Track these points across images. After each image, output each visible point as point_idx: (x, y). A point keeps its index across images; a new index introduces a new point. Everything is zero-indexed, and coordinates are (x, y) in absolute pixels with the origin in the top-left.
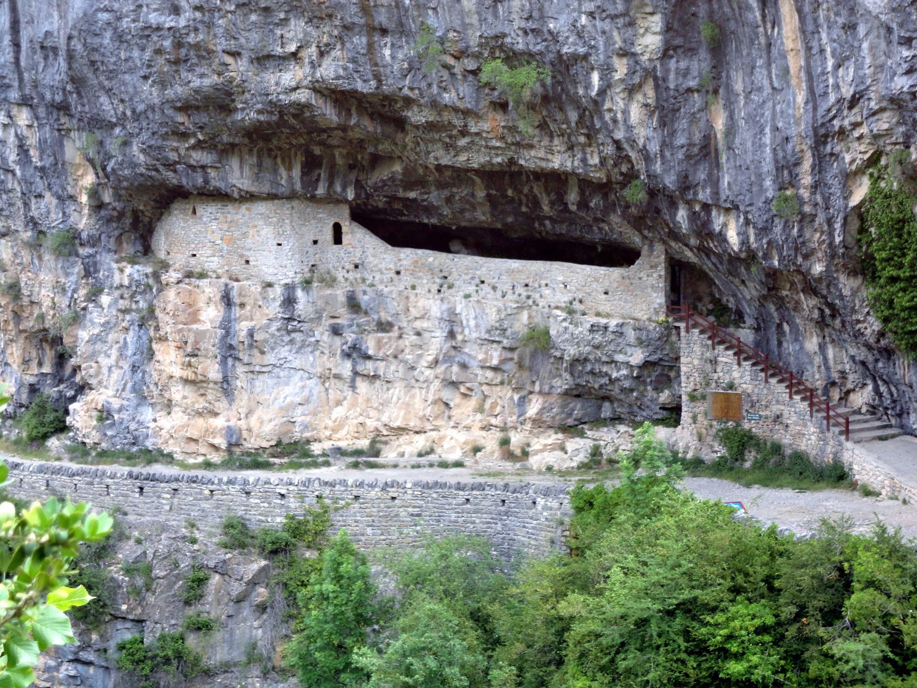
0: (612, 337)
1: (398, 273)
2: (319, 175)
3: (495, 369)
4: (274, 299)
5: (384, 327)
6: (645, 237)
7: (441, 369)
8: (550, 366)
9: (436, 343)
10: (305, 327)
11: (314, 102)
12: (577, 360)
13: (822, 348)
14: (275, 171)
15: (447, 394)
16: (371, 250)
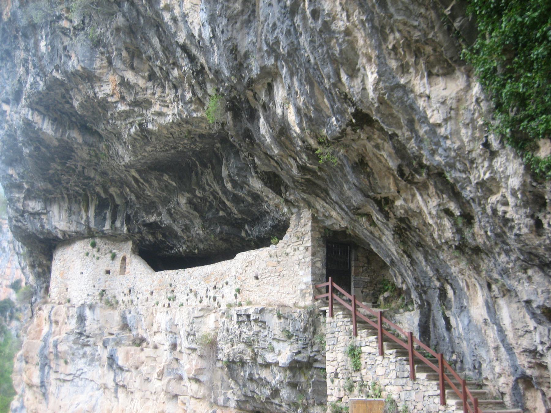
0: (256, 328)
1: (152, 293)
2: (106, 213)
3: (197, 381)
4: (72, 316)
5: (140, 342)
7: (165, 380)
8: (220, 372)
9: (165, 356)
10: (92, 340)
11: (30, 117)
12: (233, 362)
13: (492, 308)
14: (79, 213)
16: (139, 276)
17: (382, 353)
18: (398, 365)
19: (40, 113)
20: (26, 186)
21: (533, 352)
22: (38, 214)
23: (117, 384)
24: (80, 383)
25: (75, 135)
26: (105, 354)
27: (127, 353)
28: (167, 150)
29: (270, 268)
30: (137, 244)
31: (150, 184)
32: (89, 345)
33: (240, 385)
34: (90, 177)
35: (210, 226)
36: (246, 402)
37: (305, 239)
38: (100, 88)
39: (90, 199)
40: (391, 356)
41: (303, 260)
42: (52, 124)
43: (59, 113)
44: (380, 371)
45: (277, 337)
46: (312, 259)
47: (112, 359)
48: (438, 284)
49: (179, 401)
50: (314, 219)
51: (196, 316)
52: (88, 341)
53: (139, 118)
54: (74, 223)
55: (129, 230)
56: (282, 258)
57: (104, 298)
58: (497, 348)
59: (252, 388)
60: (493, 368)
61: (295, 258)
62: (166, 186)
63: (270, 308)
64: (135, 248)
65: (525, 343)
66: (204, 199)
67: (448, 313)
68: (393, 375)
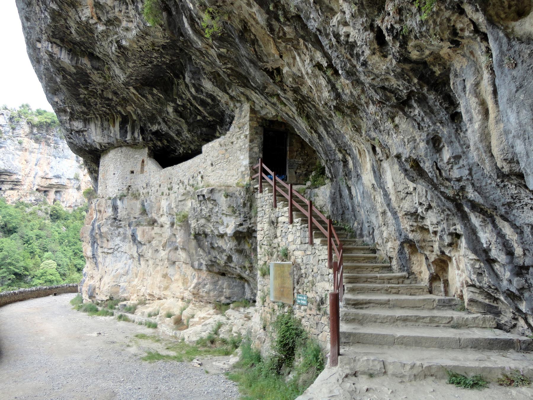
2: (127, 127)
6: (232, 98)
10: (123, 223)
11: (50, 49)
12: (199, 234)
13: (378, 173)
15: (171, 271)
17: (291, 222)
18: (302, 231)
19: (58, 45)
20: (69, 110)
21: (414, 215)
22: (82, 132)
23: (139, 255)
24: (118, 255)
25: (85, 62)
26: (129, 233)
27: (143, 231)
28: (145, 65)
29: (221, 156)
30: (152, 150)
31: (146, 98)
32: (121, 227)
33: (206, 252)
34: (108, 98)
35: (193, 129)
36: (212, 265)
37: (245, 129)
38: (82, 12)
39: (115, 117)
40: (298, 224)
41: (243, 147)
42: (69, 54)
43: (72, 45)
44: (291, 238)
45: (224, 212)
46: (250, 145)
47: (133, 236)
48: (340, 156)
49: (176, 266)
50: (253, 111)
51: (180, 200)
52: (120, 224)
53: (116, 36)
54: (106, 136)
55: (143, 139)
56: (229, 147)
57: (130, 191)
58: (384, 213)
59: (214, 255)
60: (382, 233)
61: (238, 145)
62: (159, 99)
63: (219, 188)
64: (151, 153)
65: (407, 205)
66: (184, 106)
67: (349, 183)
68: (298, 241)
